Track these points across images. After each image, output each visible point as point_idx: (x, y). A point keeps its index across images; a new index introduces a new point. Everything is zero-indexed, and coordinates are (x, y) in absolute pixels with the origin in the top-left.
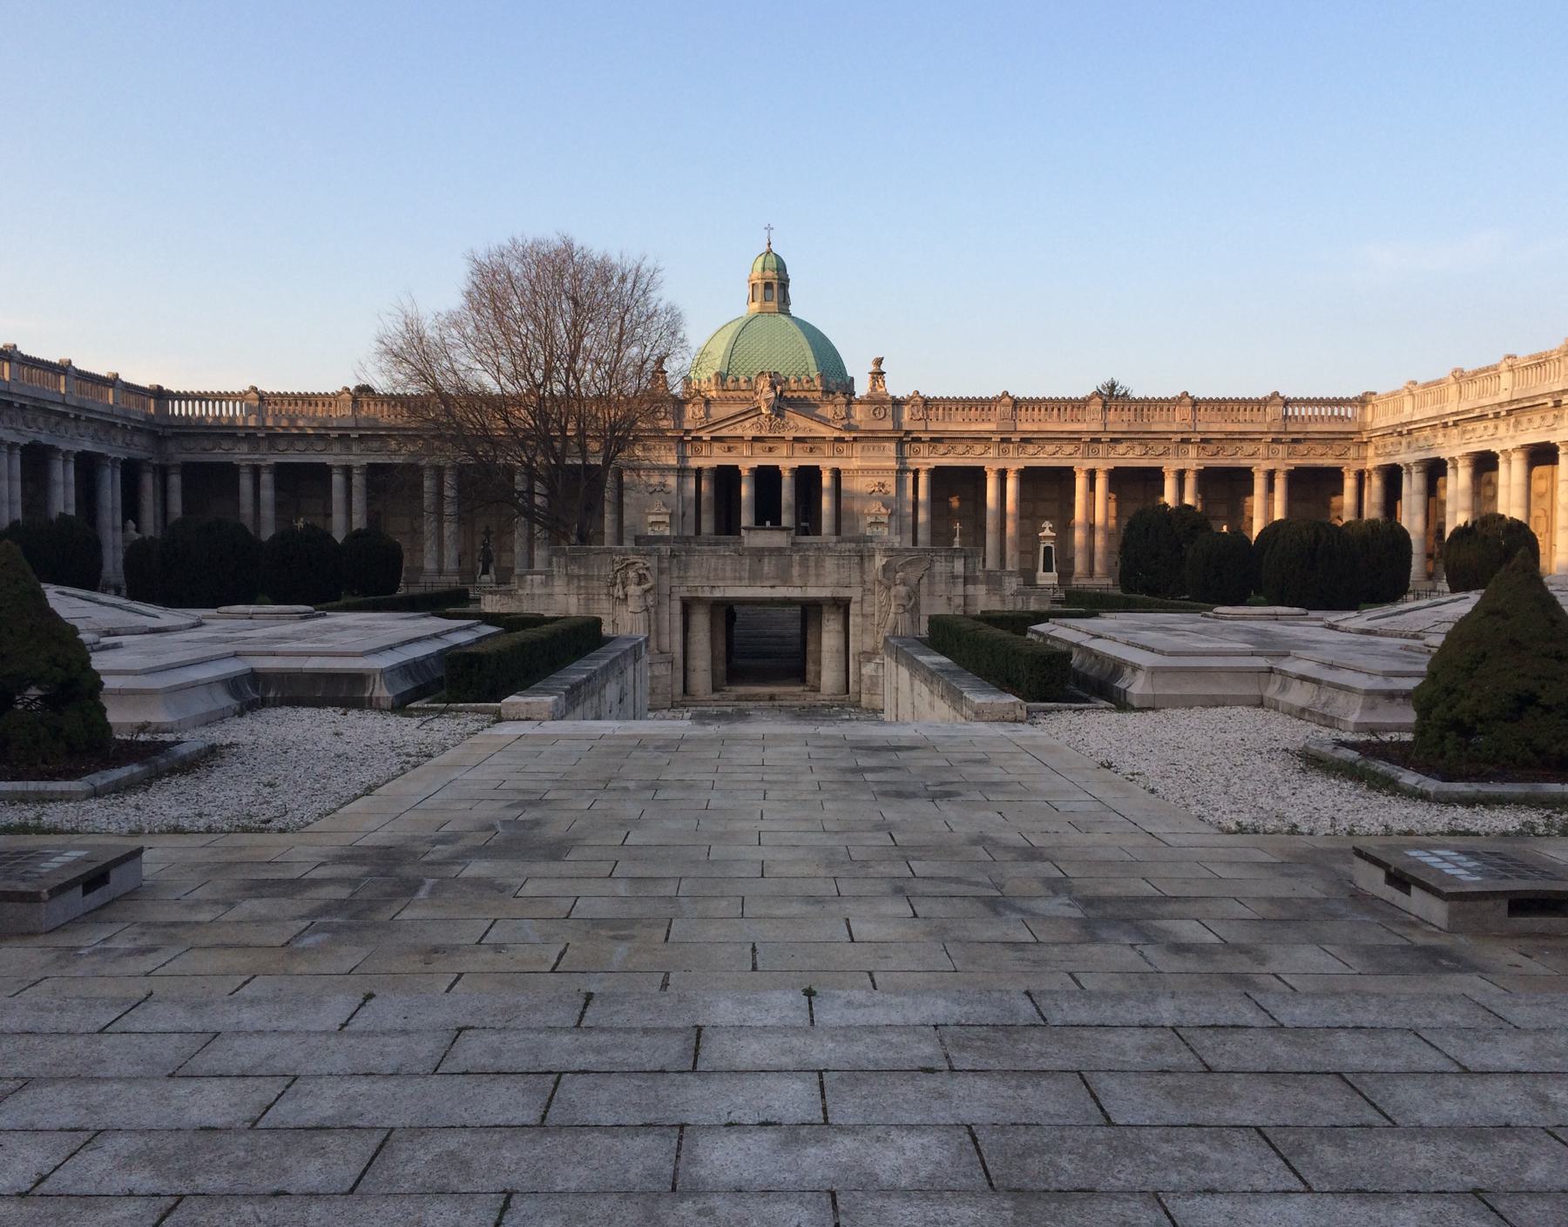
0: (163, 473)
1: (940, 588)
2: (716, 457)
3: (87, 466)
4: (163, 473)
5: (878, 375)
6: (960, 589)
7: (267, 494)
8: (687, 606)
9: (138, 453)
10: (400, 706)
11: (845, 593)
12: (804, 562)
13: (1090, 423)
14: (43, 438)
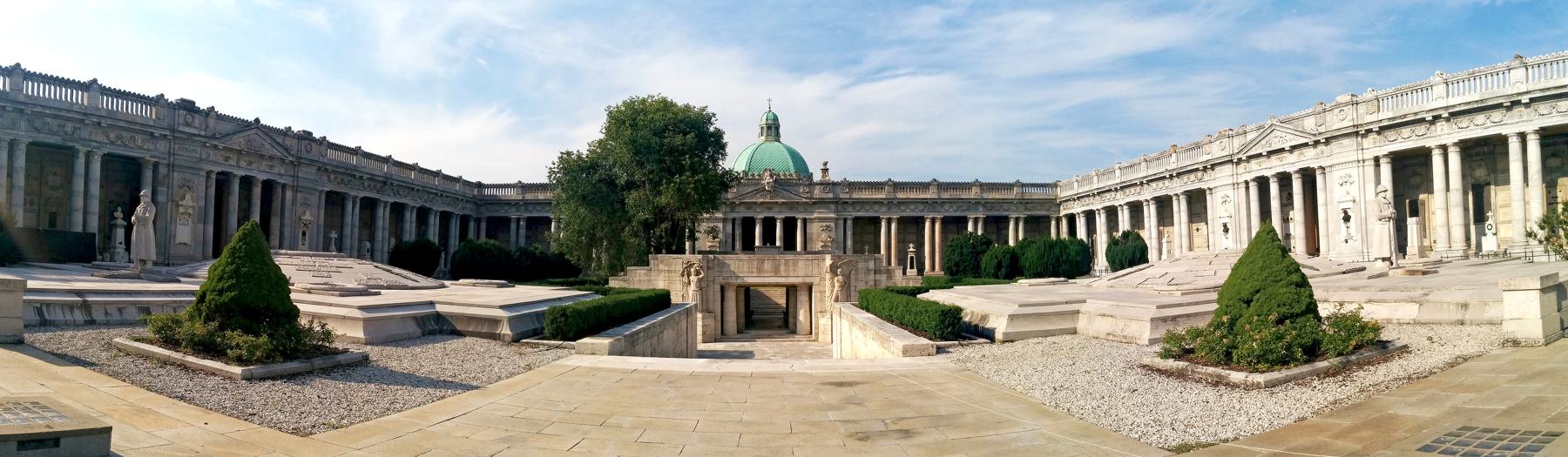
0: (478, 221)
1: (861, 276)
2: (742, 213)
3: (445, 217)
4: (478, 221)
5: (825, 171)
6: (872, 277)
7: (523, 231)
8: (723, 289)
9: (467, 212)
10: (516, 340)
11: (808, 280)
12: (786, 265)
13: (931, 194)
14: (428, 205)
